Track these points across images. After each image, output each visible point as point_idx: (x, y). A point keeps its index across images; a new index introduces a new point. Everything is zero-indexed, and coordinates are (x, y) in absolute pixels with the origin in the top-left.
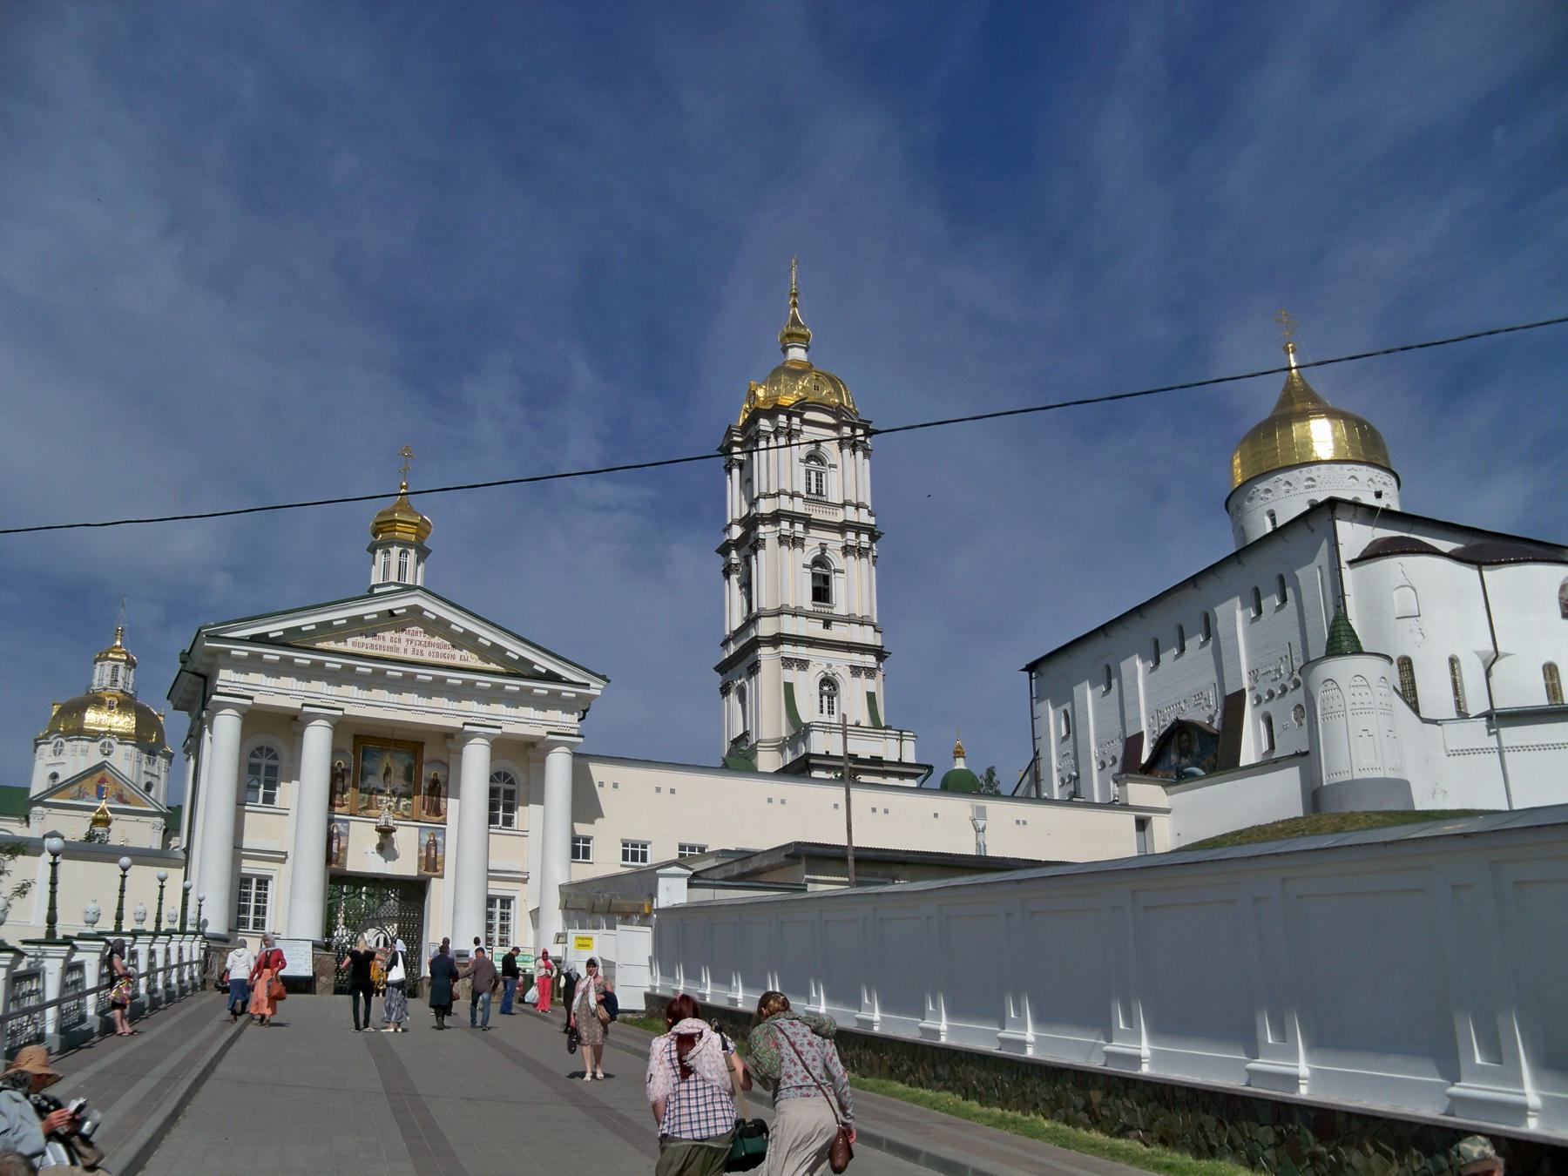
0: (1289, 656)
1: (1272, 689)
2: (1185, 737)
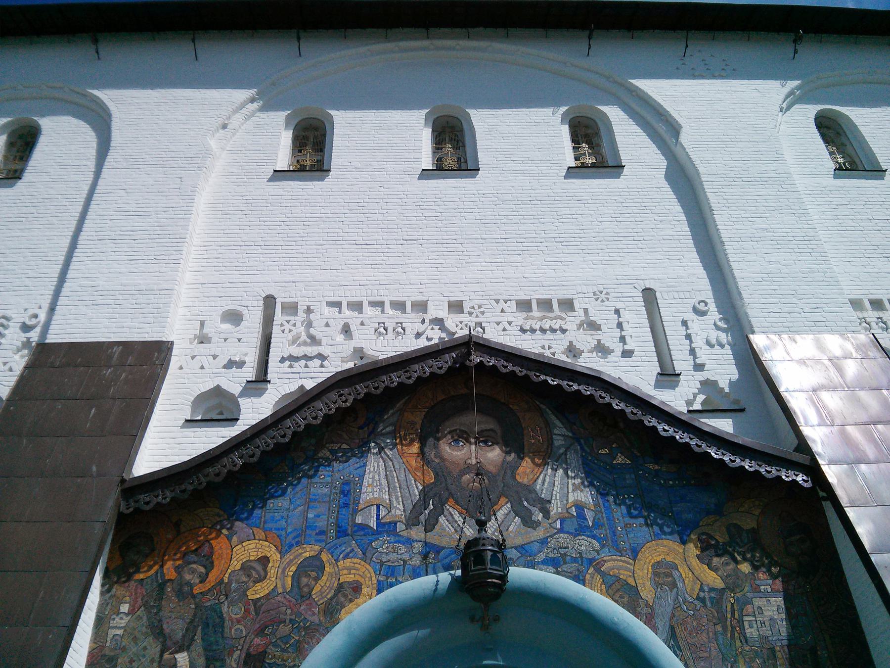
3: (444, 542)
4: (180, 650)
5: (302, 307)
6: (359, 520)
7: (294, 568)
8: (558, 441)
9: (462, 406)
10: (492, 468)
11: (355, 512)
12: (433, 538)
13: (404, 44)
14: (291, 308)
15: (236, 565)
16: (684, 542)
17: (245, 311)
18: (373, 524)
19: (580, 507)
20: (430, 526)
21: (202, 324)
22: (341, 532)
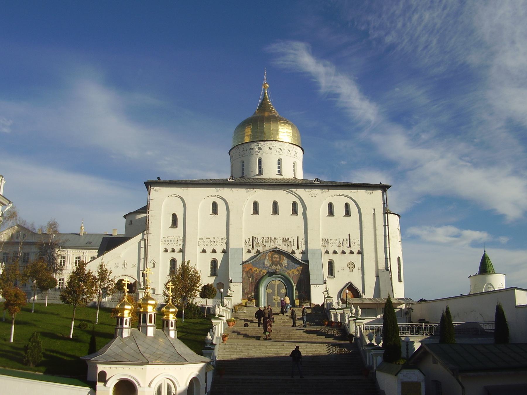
2: (276, 256)
3: (273, 269)
5: (257, 238)
7: (259, 271)
10: (278, 261)
12: (272, 268)
15: (254, 270)
16: (295, 269)
19: (286, 265)
21: (246, 240)
22: (263, 267)
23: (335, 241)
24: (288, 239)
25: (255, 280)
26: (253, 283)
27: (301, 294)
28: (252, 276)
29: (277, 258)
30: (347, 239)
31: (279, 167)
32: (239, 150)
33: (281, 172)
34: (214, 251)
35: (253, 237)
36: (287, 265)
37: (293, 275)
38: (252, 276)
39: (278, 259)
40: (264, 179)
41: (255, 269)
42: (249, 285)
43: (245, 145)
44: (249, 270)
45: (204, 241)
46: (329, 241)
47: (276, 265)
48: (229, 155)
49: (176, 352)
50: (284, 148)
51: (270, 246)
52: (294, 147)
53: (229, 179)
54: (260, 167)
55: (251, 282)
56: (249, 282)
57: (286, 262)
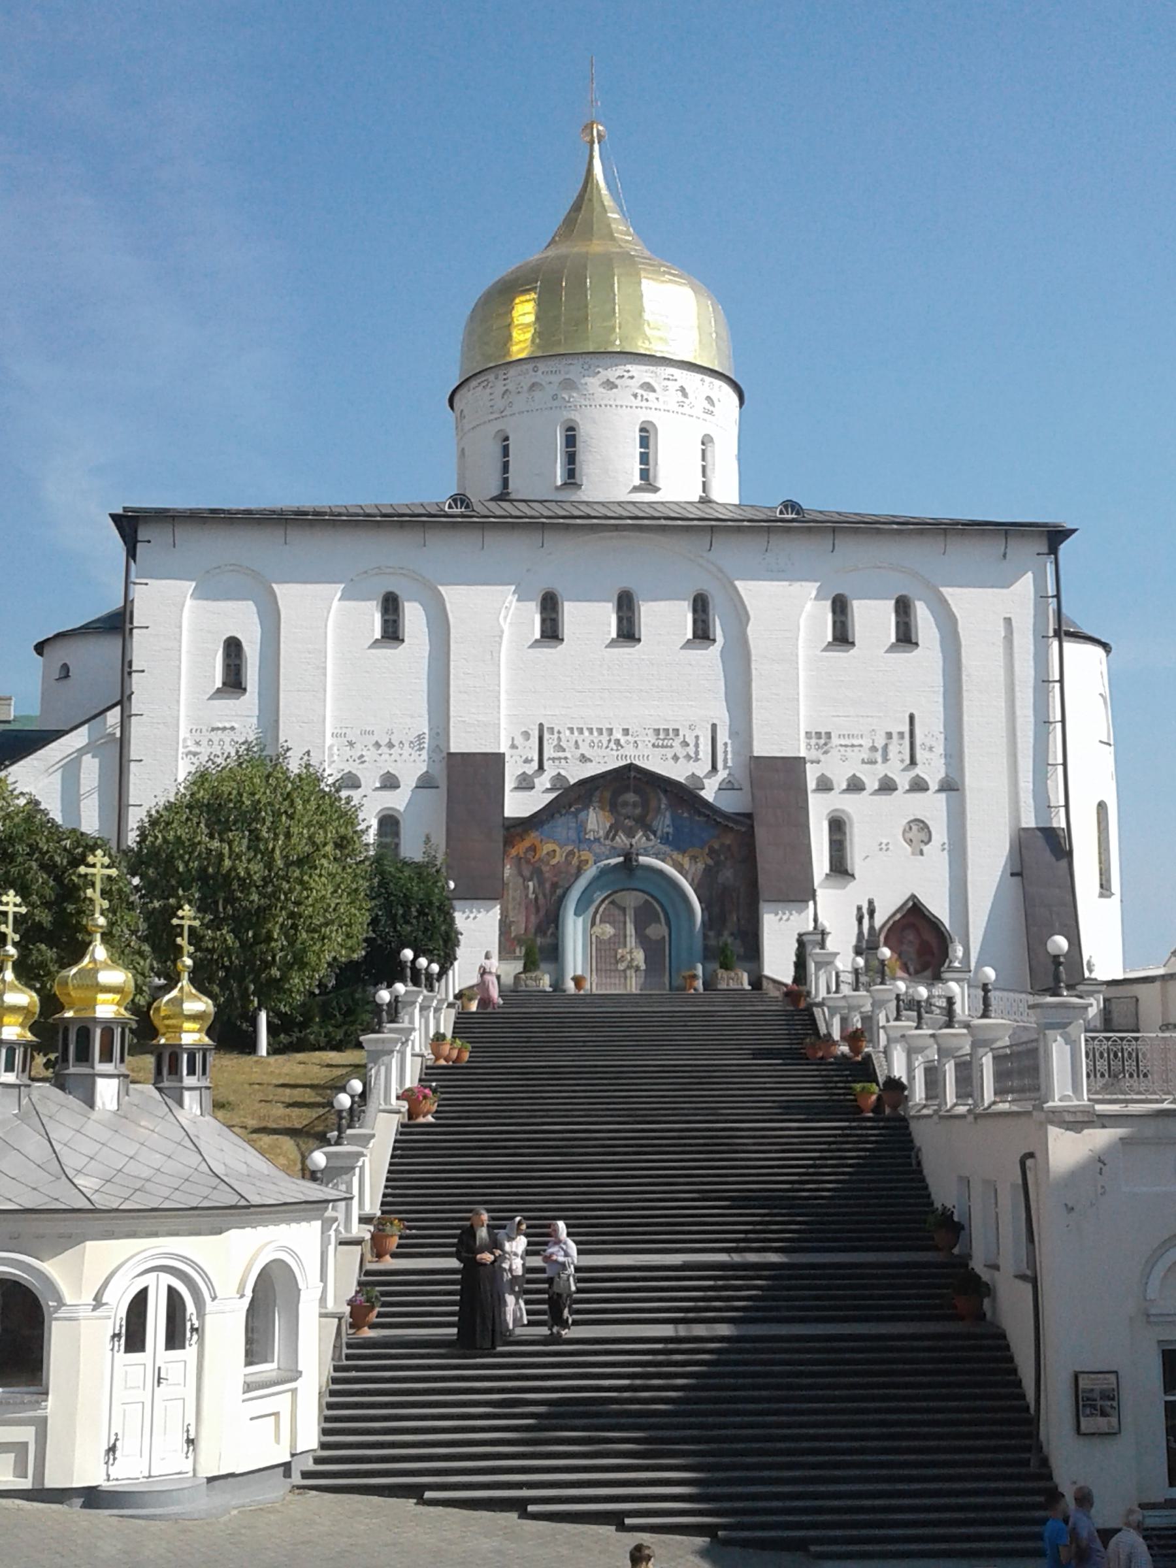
0: (907, 736)
1: (858, 774)
2: (631, 797)
4: (530, 880)
5: (556, 730)
6: (587, 837)
7: (564, 855)
8: (663, 806)
9: (627, 789)
11: (586, 834)
13: (601, 534)
14: (551, 730)
15: (545, 852)
16: (702, 848)
17: (530, 732)
18: (592, 838)
19: (668, 833)
20: (613, 839)
22: (580, 842)
23: (856, 742)
24: (676, 731)
25: (547, 891)
26: (541, 901)
27: (723, 939)
28: (537, 873)
29: (635, 805)
30: (901, 735)
31: (644, 458)
32: (488, 391)
33: (655, 477)
34: (390, 783)
35: (541, 725)
36: (671, 830)
37: (693, 870)
38: (537, 873)
39: (638, 811)
40: (587, 503)
41: (548, 847)
42: (527, 908)
43: (512, 372)
44: (525, 853)
45: (351, 744)
46: (835, 741)
47: (630, 834)
48: (449, 408)
49: (204, 1167)
50: (666, 383)
51: (605, 762)
52: (702, 380)
53: (450, 504)
54: (571, 458)
55: (534, 896)
56: (527, 896)
57: (668, 822)
